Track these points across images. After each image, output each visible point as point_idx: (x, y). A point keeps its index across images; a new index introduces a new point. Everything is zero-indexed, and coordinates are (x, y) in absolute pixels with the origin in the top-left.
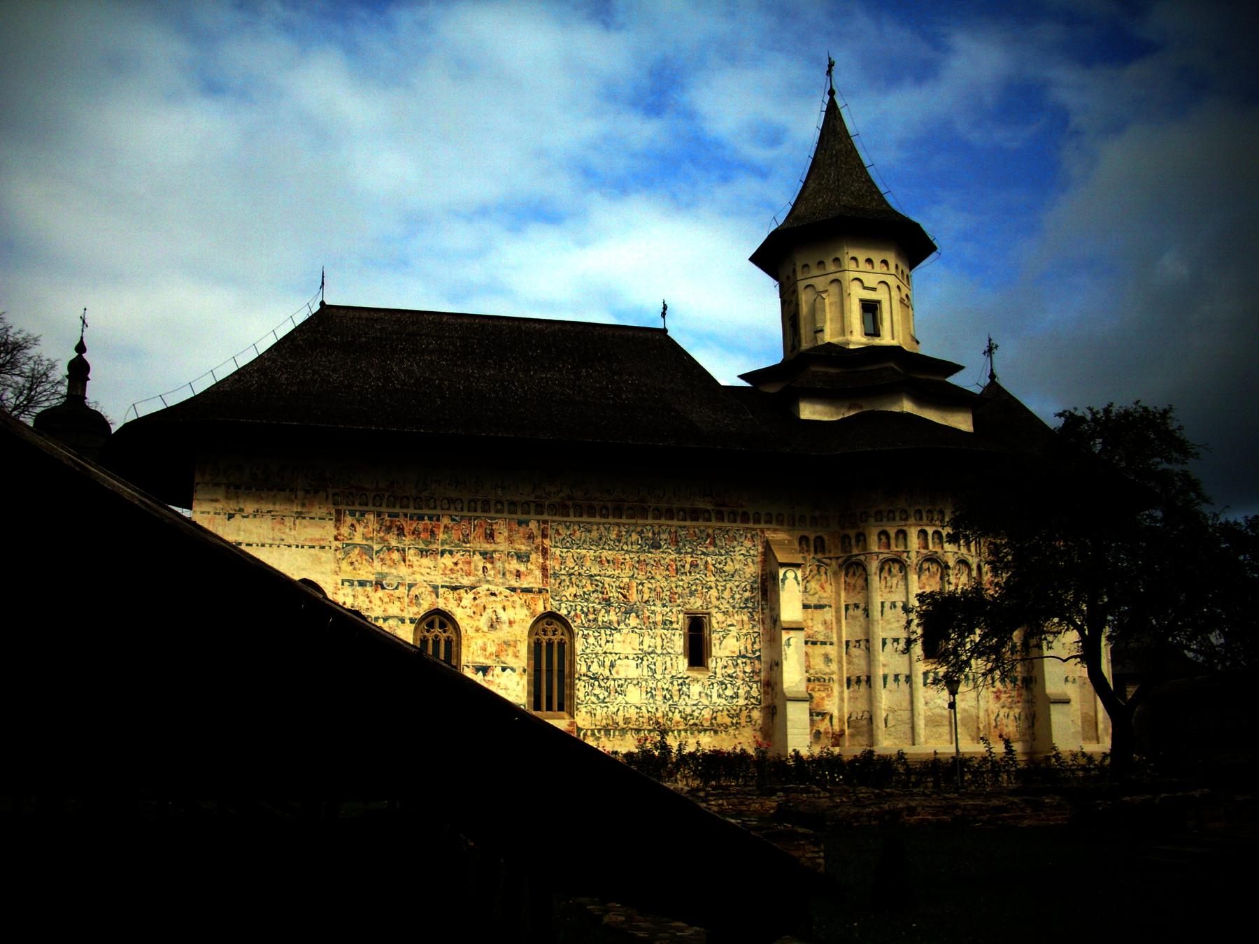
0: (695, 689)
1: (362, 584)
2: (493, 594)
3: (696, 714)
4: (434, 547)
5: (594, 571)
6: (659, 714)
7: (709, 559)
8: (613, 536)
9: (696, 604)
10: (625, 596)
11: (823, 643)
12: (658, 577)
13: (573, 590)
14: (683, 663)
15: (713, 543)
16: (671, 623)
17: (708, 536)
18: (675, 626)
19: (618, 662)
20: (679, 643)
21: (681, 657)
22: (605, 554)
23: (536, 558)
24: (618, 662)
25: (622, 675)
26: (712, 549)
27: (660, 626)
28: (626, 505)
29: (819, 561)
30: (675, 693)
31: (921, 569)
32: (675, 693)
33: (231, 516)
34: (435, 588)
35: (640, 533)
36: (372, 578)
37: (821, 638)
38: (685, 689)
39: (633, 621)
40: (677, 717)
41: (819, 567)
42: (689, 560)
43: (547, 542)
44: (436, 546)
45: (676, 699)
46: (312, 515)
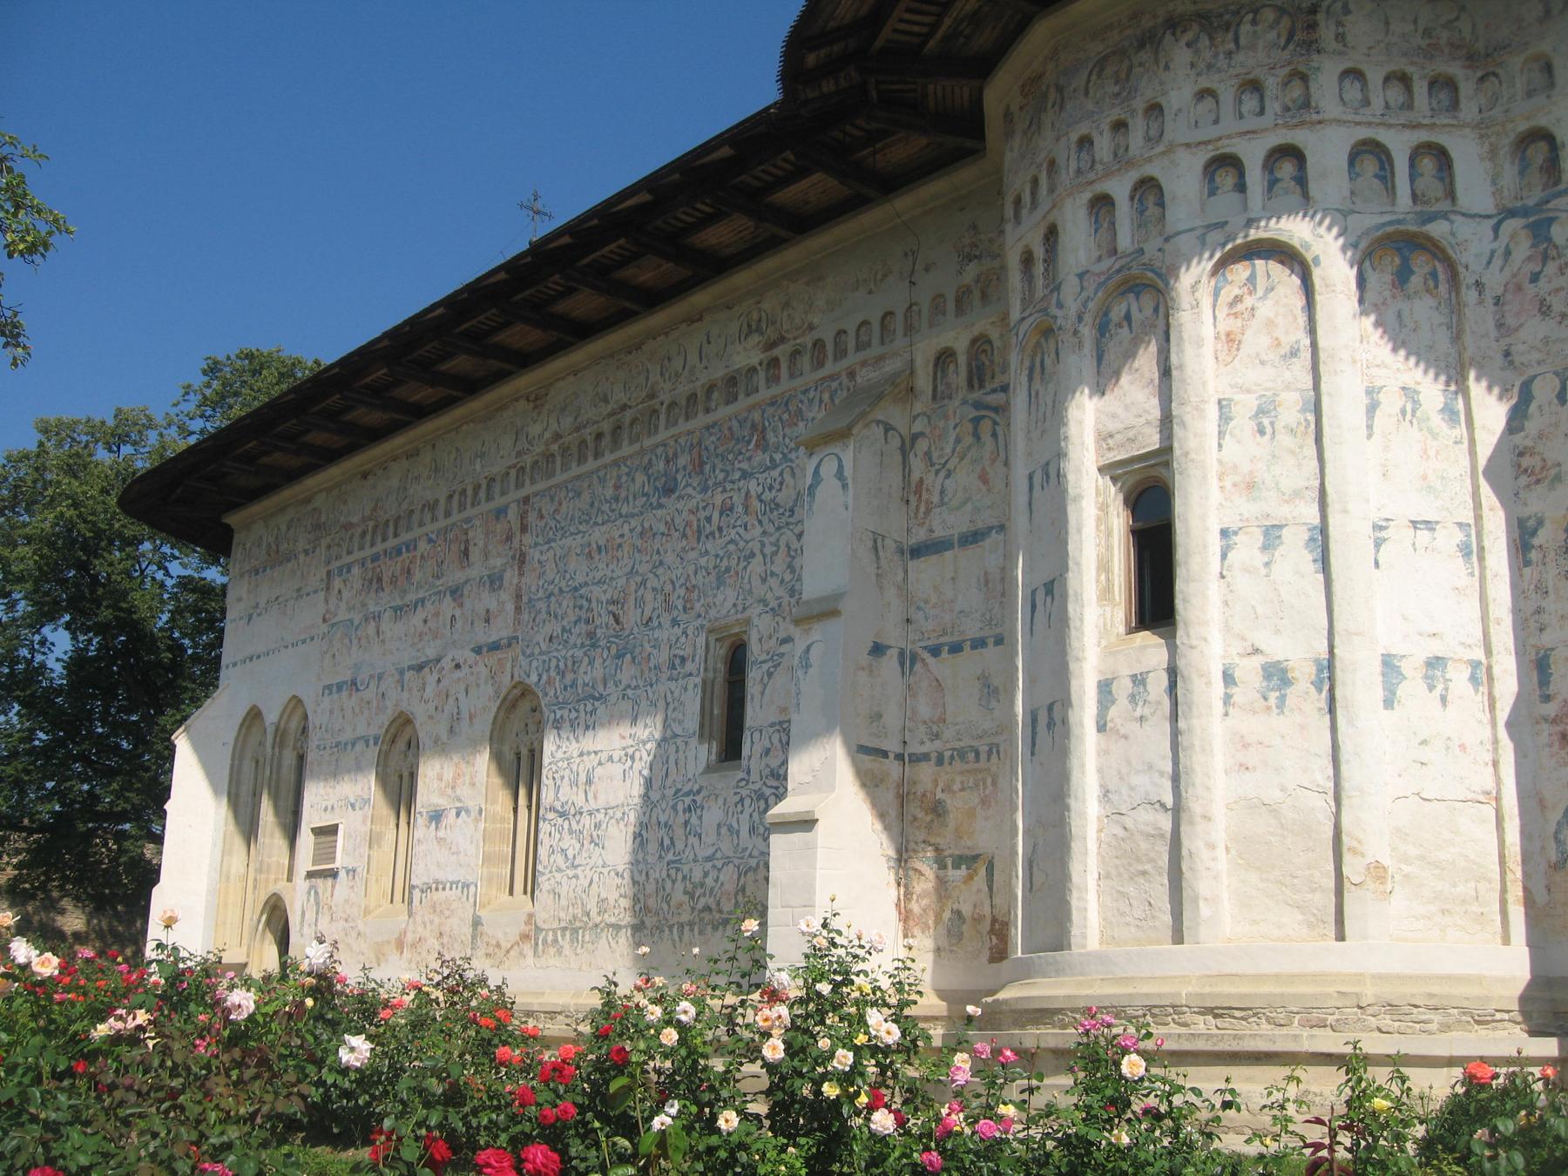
0: (713, 815)
1: (340, 687)
3: (709, 881)
4: (411, 597)
5: (580, 579)
6: (651, 888)
7: (753, 486)
8: (610, 492)
9: (724, 603)
10: (617, 621)
11: (979, 643)
12: (670, 558)
15: (763, 445)
16: (683, 660)
17: (754, 426)
18: (689, 667)
19: (599, 771)
21: (694, 742)
22: (598, 536)
23: (510, 577)
24: (599, 771)
25: (601, 803)
26: (760, 457)
27: (666, 673)
28: (628, 415)
29: (977, 405)
31: (1103, 329)
37: (972, 629)
38: (694, 820)
40: (679, 896)
41: (976, 421)
43: (528, 539)
45: (680, 845)
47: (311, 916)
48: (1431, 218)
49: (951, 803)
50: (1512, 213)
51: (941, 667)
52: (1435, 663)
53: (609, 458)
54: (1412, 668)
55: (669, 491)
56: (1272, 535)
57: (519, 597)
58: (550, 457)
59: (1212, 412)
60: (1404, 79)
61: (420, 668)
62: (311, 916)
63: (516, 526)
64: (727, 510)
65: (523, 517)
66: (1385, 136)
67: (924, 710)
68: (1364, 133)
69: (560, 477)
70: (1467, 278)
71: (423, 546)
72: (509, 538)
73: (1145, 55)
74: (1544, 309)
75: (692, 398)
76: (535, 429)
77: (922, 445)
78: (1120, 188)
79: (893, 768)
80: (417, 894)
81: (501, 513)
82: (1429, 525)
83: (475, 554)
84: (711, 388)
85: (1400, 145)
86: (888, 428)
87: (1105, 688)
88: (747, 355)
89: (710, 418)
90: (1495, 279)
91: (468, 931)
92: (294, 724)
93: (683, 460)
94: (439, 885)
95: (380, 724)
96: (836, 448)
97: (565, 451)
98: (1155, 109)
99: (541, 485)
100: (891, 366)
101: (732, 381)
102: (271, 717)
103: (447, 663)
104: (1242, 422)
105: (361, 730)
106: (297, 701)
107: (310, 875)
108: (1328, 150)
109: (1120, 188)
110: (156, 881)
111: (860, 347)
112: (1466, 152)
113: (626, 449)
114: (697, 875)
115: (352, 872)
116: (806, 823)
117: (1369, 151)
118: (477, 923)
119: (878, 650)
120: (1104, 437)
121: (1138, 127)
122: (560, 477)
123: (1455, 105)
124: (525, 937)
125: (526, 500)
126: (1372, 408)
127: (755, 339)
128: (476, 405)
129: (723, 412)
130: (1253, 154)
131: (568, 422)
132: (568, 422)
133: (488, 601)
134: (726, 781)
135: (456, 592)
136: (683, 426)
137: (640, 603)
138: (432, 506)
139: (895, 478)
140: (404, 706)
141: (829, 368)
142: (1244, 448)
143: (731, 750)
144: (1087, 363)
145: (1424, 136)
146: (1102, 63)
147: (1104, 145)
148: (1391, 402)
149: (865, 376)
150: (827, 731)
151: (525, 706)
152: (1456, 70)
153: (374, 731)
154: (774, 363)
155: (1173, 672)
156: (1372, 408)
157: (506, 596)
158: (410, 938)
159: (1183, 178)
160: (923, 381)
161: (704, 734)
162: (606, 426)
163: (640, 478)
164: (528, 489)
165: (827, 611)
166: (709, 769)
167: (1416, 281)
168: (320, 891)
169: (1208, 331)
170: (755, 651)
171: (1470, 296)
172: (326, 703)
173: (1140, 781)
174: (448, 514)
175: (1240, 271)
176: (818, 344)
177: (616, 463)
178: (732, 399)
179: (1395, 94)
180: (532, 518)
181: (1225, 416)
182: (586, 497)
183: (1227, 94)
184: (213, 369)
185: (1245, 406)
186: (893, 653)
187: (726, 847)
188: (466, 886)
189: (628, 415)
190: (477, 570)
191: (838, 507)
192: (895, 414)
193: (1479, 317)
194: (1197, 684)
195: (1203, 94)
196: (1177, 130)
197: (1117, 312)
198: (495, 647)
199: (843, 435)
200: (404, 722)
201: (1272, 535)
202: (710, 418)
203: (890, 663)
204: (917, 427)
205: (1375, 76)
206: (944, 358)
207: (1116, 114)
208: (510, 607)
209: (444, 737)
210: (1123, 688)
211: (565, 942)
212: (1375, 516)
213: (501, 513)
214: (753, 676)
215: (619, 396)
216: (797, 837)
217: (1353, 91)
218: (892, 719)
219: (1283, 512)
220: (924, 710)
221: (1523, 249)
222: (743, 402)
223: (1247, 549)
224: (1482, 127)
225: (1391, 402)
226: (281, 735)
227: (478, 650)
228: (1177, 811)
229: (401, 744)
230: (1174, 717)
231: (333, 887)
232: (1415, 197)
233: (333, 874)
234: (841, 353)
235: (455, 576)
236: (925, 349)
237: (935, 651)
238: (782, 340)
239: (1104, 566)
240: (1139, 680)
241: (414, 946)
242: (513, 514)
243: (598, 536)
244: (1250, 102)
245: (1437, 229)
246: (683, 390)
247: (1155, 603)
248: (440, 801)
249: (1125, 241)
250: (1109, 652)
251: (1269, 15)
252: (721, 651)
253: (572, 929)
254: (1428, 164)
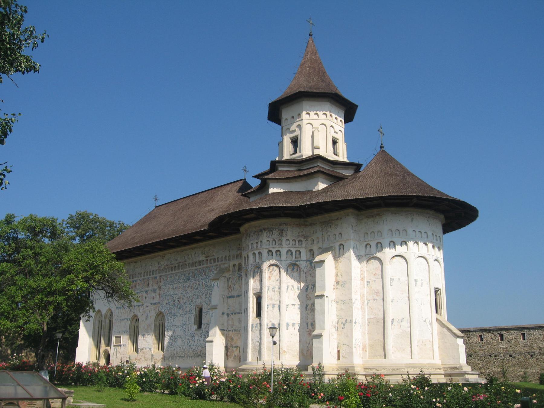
0: (197, 338)
5: (172, 293)
6: (186, 350)
8: (177, 278)
9: (199, 301)
11: (239, 313)
12: (189, 292)
13: (166, 302)
14: (195, 327)
15: (205, 274)
18: (192, 312)
20: (192, 319)
22: (175, 285)
23: (158, 290)
26: (204, 276)
28: (181, 264)
30: (191, 340)
31: (254, 273)
32: (191, 340)
35: (184, 275)
37: (238, 311)
39: (181, 312)
40: (191, 351)
41: (239, 277)
42: (197, 283)
43: (161, 284)
47: (115, 354)
48: (297, 261)
49: (234, 338)
50: (308, 261)
51: (233, 316)
52: (294, 324)
53: (177, 271)
54: (291, 325)
55: (189, 280)
56: (274, 306)
57: (160, 295)
58: (165, 269)
59: (267, 288)
60: (295, 240)
61: (139, 306)
62: (115, 354)
63: (159, 281)
64: (199, 285)
65: (160, 279)
66: (292, 249)
67: (231, 323)
68: (288, 249)
69: (168, 273)
70: (302, 270)
71: (139, 281)
72: (157, 283)
73: (260, 233)
74: (311, 275)
75: (193, 263)
76: (163, 263)
77: (231, 280)
78: (257, 252)
79: (225, 332)
81: (155, 278)
82: (294, 305)
83: (150, 285)
84: (196, 262)
85: (294, 250)
86: (225, 277)
87: (252, 325)
88: (202, 258)
89: (196, 268)
90: (305, 270)
91: (151, 357)
92: (109, 314)
93: (191, 274)
96: (217, 281)
97: (168, 268)
98: (261, 242)
99: (164, 274)
100: (226, 265)
101: (200, 262)
102: (104, 312)
103: (145, 306)
104: (271, 290)
105: (126, 317)
106: (110, 309)
107: (115, 346)
108: (284, 251)
109: (257, 252)
110: (77, 346)
111: (222, 261)
112: (303, 251)
113: (181, 270)
114: (194, 348)
115: (124, 345)
116: (212, 342)
117: (289, 251)
118: (152, 355)
119: (223, 314)
120: (253, 289)
121: (259, 243)
122: (168, 273)
123: (302, 244)
125: (161, 276)
126: (288, 288)
127: (204, 255)
128: (150, 256)
129: (198, 267)
130: (274, 251)
131: (169, 263)
132: (169, 263)
133: (153, 295)
134: (199, 332)
135: (146, 292)
136: (191, 268)
137: (183, 299)
138: (141, 274)
139: (226, 285)
140: (135, 313)
141: (216, 263)
142: (270, 293)
143: (200, 326)
144: (252, 275)
145: (297, 249)
146: (255, 232)
147: (255, 245)
148: (290, 288)
149: (222, 266)
150: (215, 326)
151: (161, 315)
152: (302, 239)
153: (128, 318)
154: (207, 260)
155: (260, 324)
156: (288, 288)
157: (157, 294)
159: (265, 253)
160: (231, 269)
161: (195, 324)
162: (177, 265)
163: (183, 276)
164: (161, 274)
165: (215, 308)
166: (196, 330)
167: (295, 270)
169: (267, 276)
170: (204, 310)
171: (302, 272)
172: (117, 310)
173: (256, 338)
174: (144, 276)
175: (271, 268)
176: (215, 259)
177: (179, 273)
178: (200, 265)
179: (294, 243)
180: (162, 280)
181: (268, 289)
182: (173, 278)
183: (271, 242)
184: (71, 217)
185: (271, 287)
186: (225, 315)
187: (199, 343)
188: (150, 349)
189: (181, 264)
190: (151, 288)
191: (218, 291)
192: (227, 275)
193: (303, 275)
194: (263, 326)
195: (268, 241)
196: (264, 246)
197: (256, 270)
198: (155, 304)
199: (218, 279)
200: (135, 316)
201: (274, 306)
202: (196, 268)
203: (225, 315)
204: (230, 276)
205: (291, 240)
206: (234, 265)
207: (256, 241)
208: (158, 297)
210: (255, 325)
211: (170, 359)
212: (287, 304)
213: (155, 278)
214: (203, 315)
215: (179, 260)
216: (210, 344)
217: (288, 242)
218: (225, 324)
219: (275, 303)
220: (231, 323)
221: (309, 266)
222: (202, 266)
223: (270, 308)
224: (305, 248)
225: (290, 288)
226: (106, 316)
227: (151, 304)
228: (260, 343)
229: (135, 320)
230: (260, 330)
232: (295, 258)
233: (120, 346)
234: (218, 261)
235: (146, 289)
236: (232, 263)
237: (232, 314)
238: (208, 257)
239: (253, 308)
240: (257, 325)
241: (139, 360)
242: (158, 278)
243: (175, 285)
244: (274, 242)
245: (298, 263)
246: (191, 262)
247: (259, 314)
249: (257, 261)
250: (253, 320)
251: (277, 230)
252: (198, 309)
253: (171, 357)
254: (298, 252)
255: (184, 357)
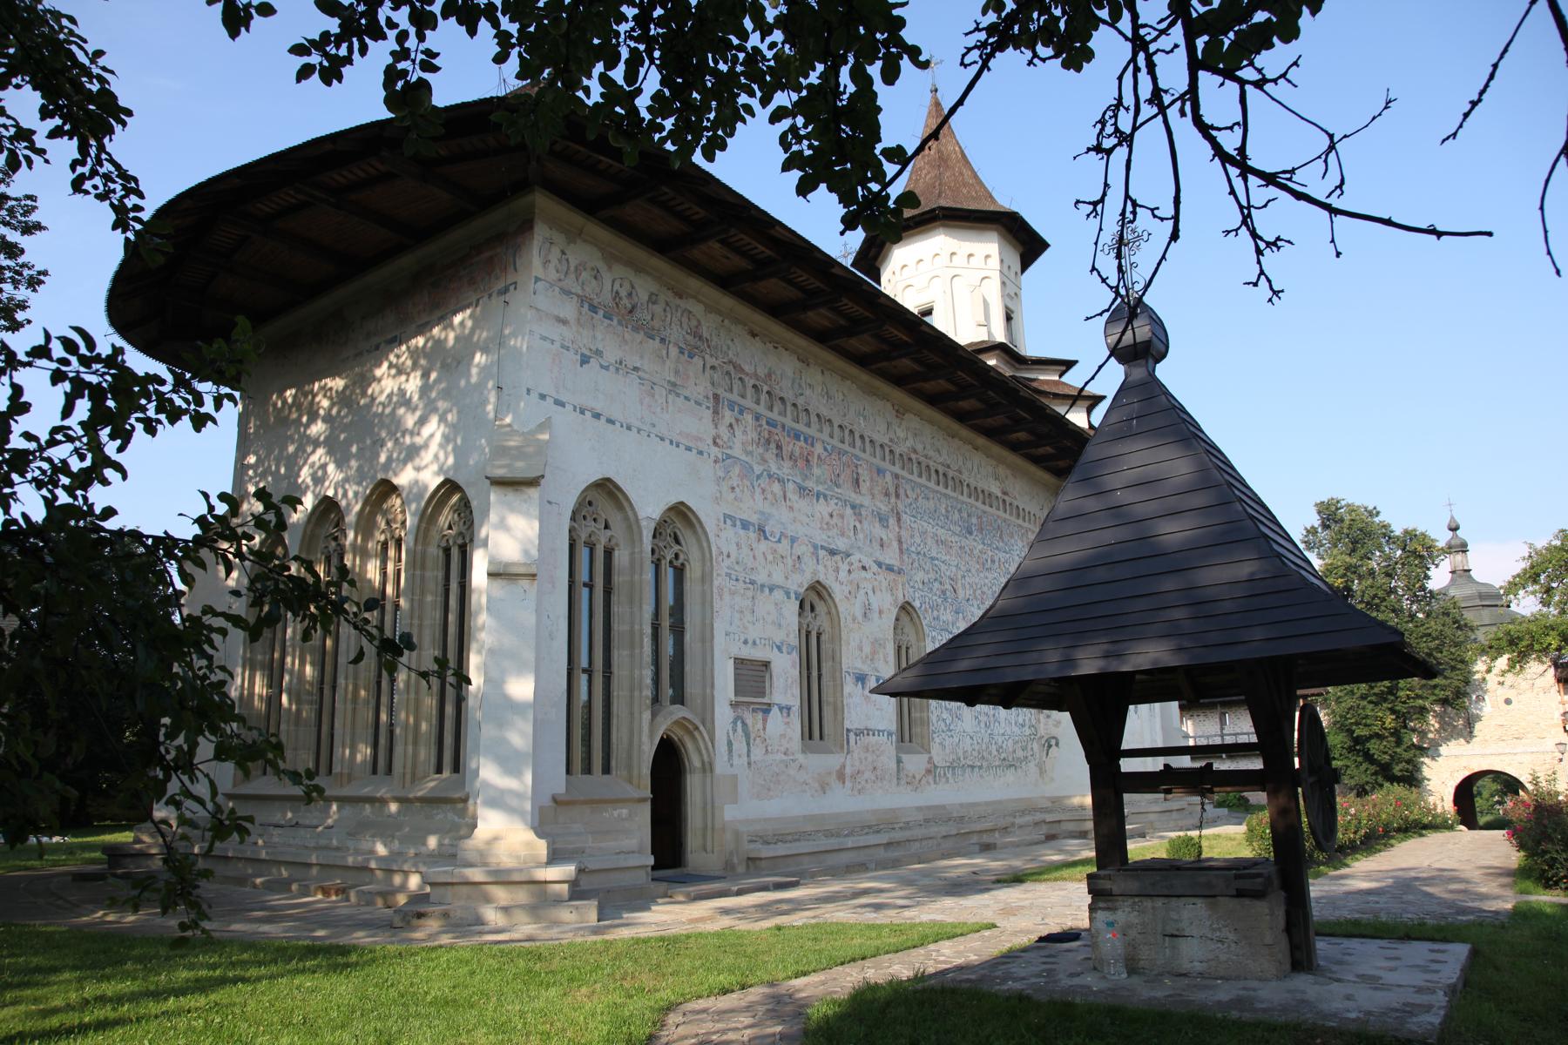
2: (864, 568)
33: (585, 360)
34: (815, 547)
36: (754, 519)
44: (810, 484)
46: (687, 394)
62: (740, 745)
71: (818, 449)
80: (852, 735)
94: (868, 731)
95: (799, 582)
105: (778, 578)
124: (928, 771)
140: (822, 578)
158: (848, 771)
168: (749, 722)
209: (860, 618)
227: (880, 565)
231: (765, 720)
248: (866, 669)
255: (980, 767)
